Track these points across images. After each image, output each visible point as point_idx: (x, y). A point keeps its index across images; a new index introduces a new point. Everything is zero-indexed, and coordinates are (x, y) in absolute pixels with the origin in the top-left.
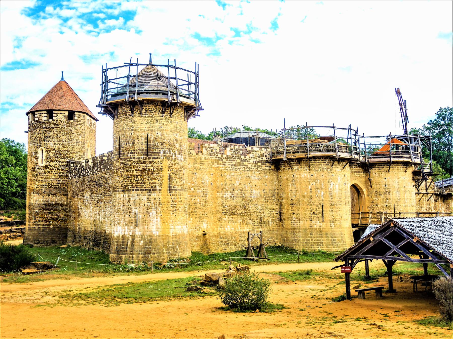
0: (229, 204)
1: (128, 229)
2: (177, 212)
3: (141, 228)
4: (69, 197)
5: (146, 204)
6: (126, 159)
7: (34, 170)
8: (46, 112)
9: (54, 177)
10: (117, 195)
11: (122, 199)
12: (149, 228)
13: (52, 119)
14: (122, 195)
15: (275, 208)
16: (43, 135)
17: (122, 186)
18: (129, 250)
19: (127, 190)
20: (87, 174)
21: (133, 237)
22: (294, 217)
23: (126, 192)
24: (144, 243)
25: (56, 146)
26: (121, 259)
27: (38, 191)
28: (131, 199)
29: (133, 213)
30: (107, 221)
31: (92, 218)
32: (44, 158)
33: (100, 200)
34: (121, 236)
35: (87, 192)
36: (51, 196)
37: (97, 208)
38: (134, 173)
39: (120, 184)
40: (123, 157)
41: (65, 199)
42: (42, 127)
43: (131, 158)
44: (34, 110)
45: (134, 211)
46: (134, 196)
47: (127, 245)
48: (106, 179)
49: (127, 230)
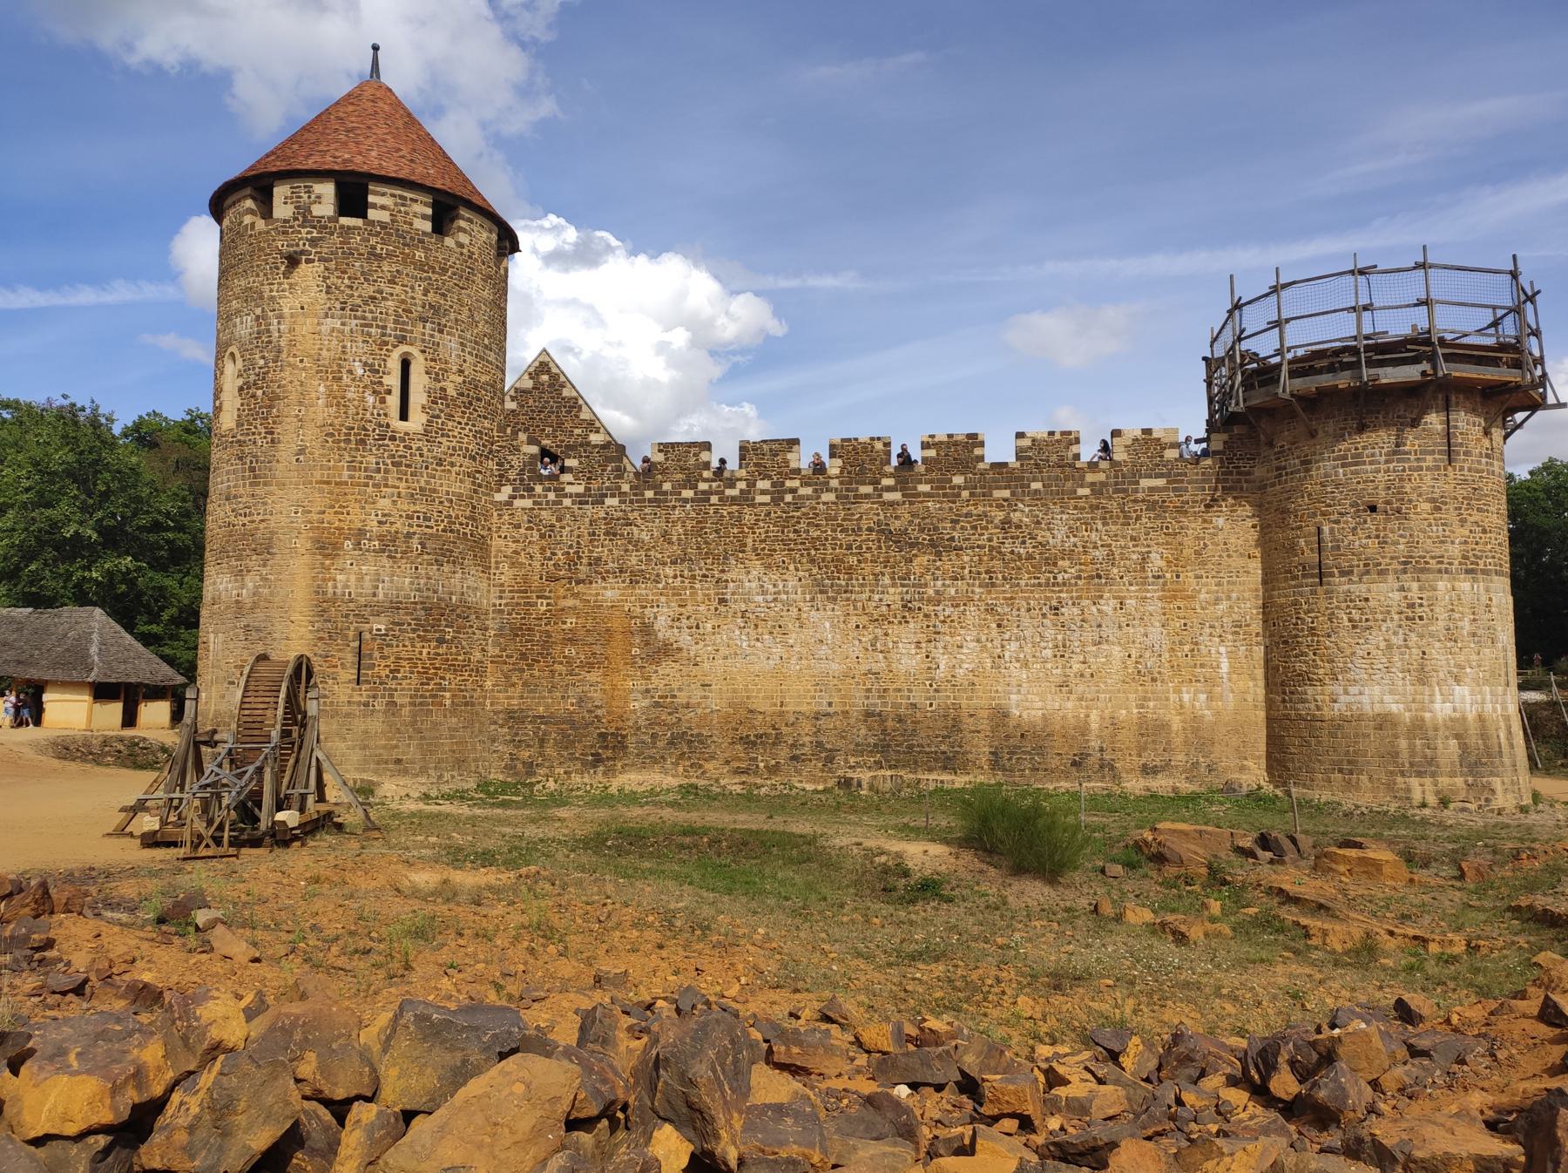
6: (1478, 471)
7: (363, 442)
10: (1441, 585)
14: (1465, 586)
16: (419, 295)
17: (1465, 557)
23: (1480, 576)
25: (468, 358)
26: (1493, 791)
31: (835, 667)
34: (1471, 716)
36: (446, 568)
39: (1455, 550)
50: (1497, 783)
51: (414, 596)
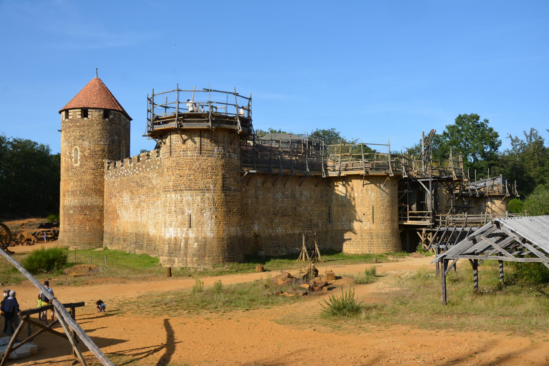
0: (280, 205)
1: (181, 230)
2: (231, 213)
3: (195, 229)
4: (105, 198)
5: (200, 205)
8: (80, 110)
9: (89, 177)
10: (168, 195)
11: (173, 200)
12: (203, 229)
13: (87, 117)
14: (173, 195)
15: (324, 209)
16: (78, 134)
17: (174, 186)
18: (182, 252)
19: (179, 190)
20: (126, 175)
21: (187, 240)
22: (344, 218)
23: (178, 192)
24: (198, 245)
26: (174, 262)
27: (73, 192)
28: (184, 199)
29: (186, 214)
30: (151, 223)
31: (132, 220)
32: (79, 158)
33: (142, 201)
34: (173, 238)
35: (126, 193)
37: (139, 210)
38: (187, 172)
39: (171, 184)
40: (174, 154)
41: (101, 200)
42: (76, 126)
43: (184, 156)
44: (68, 108)
45: (187, 211)
46: (187, 196)
47: (180, 247)
48: (149, 179)
49: (179, 231)
50: (176, 259)
51: (78, 205)
